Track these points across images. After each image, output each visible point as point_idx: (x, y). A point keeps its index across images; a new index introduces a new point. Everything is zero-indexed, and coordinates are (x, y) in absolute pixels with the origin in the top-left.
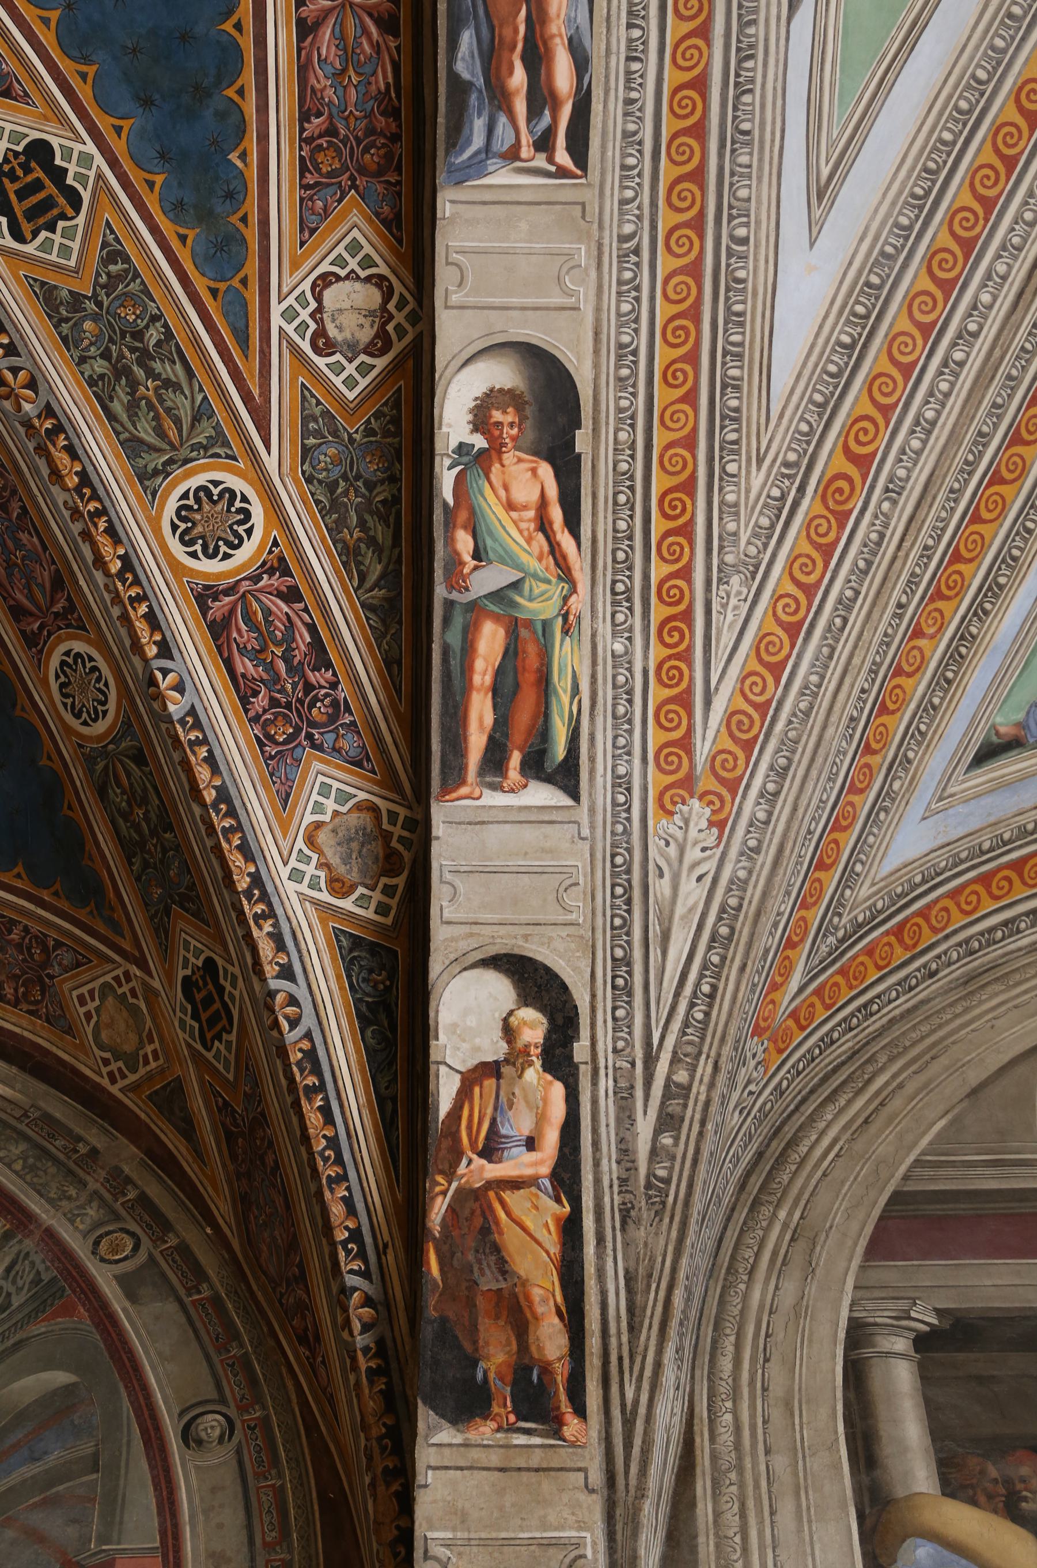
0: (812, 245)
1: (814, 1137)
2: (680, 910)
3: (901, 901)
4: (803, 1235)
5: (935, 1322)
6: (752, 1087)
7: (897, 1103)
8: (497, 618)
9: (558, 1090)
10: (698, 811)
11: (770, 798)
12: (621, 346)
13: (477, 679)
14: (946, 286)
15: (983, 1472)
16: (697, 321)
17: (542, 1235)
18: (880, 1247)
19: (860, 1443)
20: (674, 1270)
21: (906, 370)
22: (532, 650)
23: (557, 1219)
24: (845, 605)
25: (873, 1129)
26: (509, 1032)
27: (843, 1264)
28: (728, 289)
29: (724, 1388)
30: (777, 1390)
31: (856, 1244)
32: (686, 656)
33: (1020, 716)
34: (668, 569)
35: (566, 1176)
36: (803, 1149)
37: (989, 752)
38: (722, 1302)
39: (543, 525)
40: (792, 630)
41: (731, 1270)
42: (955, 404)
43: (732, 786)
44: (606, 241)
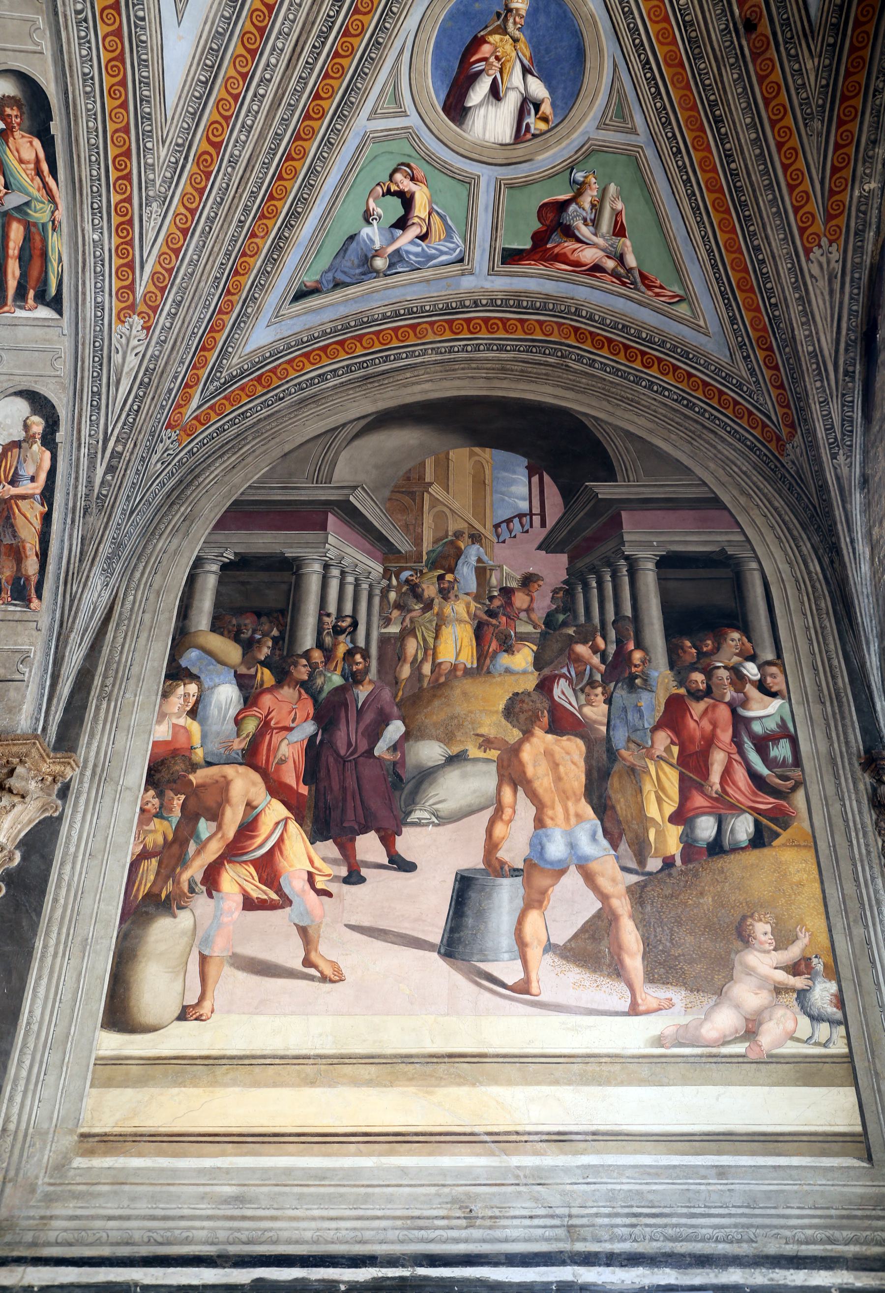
0: (179, 24)
2: (126, 370)
3: (257, 365)
4: (189, 519)
6: (171, 452)
7: (250, 459)
8: (19, 221)
9: (48, 455)
10: (137, 321)
11: (172, 316)
12: (84, 74)
13: (11, 252)
14: (253, 53)
16: (123, 63)
17: (33, 521)
18: (221, 525)
20: (102, 536)
21: (236, 97)
22: (37, 238)
23: (41, 514)
24: (211, 220)
25: (235, 471)
26: (26, 427)
28: (137, 46)
29: (133, 585)
30: (156, 586)
32: (131, 243)
33: (318, 277)
34: (120, 197)
35: (48, 495)
37: (301, 295)
38: (144, 548)
39: (39, 172)
40: (184, 232)
41: (153, 533)
42: (261, 117)
43: (154, 310)
44: (68, 13)
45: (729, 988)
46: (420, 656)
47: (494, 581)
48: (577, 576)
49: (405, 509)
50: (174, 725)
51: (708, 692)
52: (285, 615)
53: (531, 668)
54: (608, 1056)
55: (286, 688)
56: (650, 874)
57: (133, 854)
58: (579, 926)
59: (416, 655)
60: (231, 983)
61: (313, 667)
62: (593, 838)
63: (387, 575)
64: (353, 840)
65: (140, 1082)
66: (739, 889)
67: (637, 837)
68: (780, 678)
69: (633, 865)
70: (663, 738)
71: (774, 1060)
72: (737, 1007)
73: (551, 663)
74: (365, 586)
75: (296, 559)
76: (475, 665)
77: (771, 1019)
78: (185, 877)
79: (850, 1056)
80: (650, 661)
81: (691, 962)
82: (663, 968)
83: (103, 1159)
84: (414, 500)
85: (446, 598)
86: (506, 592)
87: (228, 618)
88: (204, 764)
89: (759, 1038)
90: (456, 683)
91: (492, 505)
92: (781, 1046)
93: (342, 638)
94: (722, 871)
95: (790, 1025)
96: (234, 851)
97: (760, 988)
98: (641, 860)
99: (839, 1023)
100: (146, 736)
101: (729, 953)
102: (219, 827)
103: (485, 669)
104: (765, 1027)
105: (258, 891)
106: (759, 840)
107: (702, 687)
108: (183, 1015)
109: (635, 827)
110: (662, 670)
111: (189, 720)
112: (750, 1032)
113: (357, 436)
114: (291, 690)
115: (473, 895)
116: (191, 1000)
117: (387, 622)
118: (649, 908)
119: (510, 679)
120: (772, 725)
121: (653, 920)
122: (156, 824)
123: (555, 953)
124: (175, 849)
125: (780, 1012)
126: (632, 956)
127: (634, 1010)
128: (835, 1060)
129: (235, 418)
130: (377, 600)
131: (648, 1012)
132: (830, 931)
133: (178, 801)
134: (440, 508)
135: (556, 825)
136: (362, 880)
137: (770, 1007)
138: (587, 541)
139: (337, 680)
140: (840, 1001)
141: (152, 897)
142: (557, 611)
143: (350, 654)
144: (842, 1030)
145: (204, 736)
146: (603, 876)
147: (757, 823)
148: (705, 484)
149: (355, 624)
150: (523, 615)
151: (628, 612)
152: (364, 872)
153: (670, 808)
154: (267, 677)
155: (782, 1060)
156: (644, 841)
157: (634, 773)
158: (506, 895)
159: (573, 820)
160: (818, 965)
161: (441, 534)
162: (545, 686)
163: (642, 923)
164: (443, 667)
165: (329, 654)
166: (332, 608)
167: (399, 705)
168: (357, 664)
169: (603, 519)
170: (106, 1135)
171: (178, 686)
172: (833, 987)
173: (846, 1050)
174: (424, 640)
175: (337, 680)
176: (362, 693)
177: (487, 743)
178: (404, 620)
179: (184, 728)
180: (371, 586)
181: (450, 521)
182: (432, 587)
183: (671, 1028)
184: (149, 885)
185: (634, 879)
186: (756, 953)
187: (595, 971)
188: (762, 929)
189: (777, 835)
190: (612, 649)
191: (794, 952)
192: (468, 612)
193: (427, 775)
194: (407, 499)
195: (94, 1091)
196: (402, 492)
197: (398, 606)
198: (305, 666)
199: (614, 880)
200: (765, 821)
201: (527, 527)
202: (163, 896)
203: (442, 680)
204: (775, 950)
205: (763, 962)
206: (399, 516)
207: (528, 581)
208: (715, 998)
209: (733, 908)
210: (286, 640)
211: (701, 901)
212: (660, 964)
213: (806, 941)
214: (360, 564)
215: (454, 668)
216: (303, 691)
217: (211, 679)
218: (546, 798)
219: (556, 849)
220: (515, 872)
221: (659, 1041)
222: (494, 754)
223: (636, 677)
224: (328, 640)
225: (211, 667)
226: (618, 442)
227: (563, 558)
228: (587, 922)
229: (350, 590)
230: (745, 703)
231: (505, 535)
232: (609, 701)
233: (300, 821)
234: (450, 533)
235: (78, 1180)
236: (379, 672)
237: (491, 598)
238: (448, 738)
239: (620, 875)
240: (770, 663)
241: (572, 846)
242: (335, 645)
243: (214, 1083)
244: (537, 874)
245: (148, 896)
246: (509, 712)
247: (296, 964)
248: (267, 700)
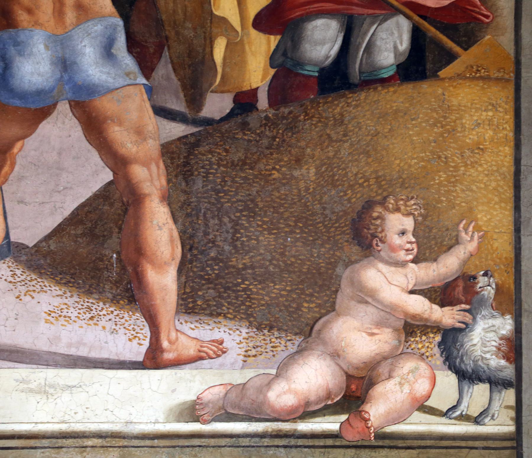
45: (325, 325)
54: (99, 435)
56: (208, 122)
58: (67, 213)
62: (108, 52)
66: (367, 154)
67: (191, 52)
69: (178, 105)
71: (387, 442)
72: (335, 355)
77: (390, 377)
81: (265, 278)
82: (209, 290)
89: (367, 407)
92: (401, 419)
94: (340, 121)
95: (422, 387)
97: (380, 324)
98: (195, 96)
99: (506, 384)
101: (333, 265)
104: (379, 389)
106: (417, 65)
109: (189, 33)
118: (199, 184)
121: (204, 206)
123: (17, 260)
125: (407, 366)
126: (160, 267)
127: (154, 360)
128: (490, 444)
131: (177, 363)
132: (517, 230)
135: (37, 24)
137: (392, 357)
140: (513, 348)
144: (509, 396)
146: (120, 124)
147: (417, 34)
155: (400, 443)
156: (203, 62)
159: (70, 16)
160: (486, 288)
163: (184, 212)
172: (505, 325)
173: (512, 428)
183: (216, 390)
185: (176, 130)
186: (381, 266)
187: (89, 293)
188: (398, 226)
189: (451, 57)
191: (449, 265)
199: (139, 132)
200: (432, 31)
204: (415, 261)
205: (392, 281)
208: (298, 340)
209: (351, 187)
211: (296, 173)
212: (209, 281)
213: (472, 246)
221: (192, 411)
228: (82, 206)
239: (151, 121)
241: (65, 65)
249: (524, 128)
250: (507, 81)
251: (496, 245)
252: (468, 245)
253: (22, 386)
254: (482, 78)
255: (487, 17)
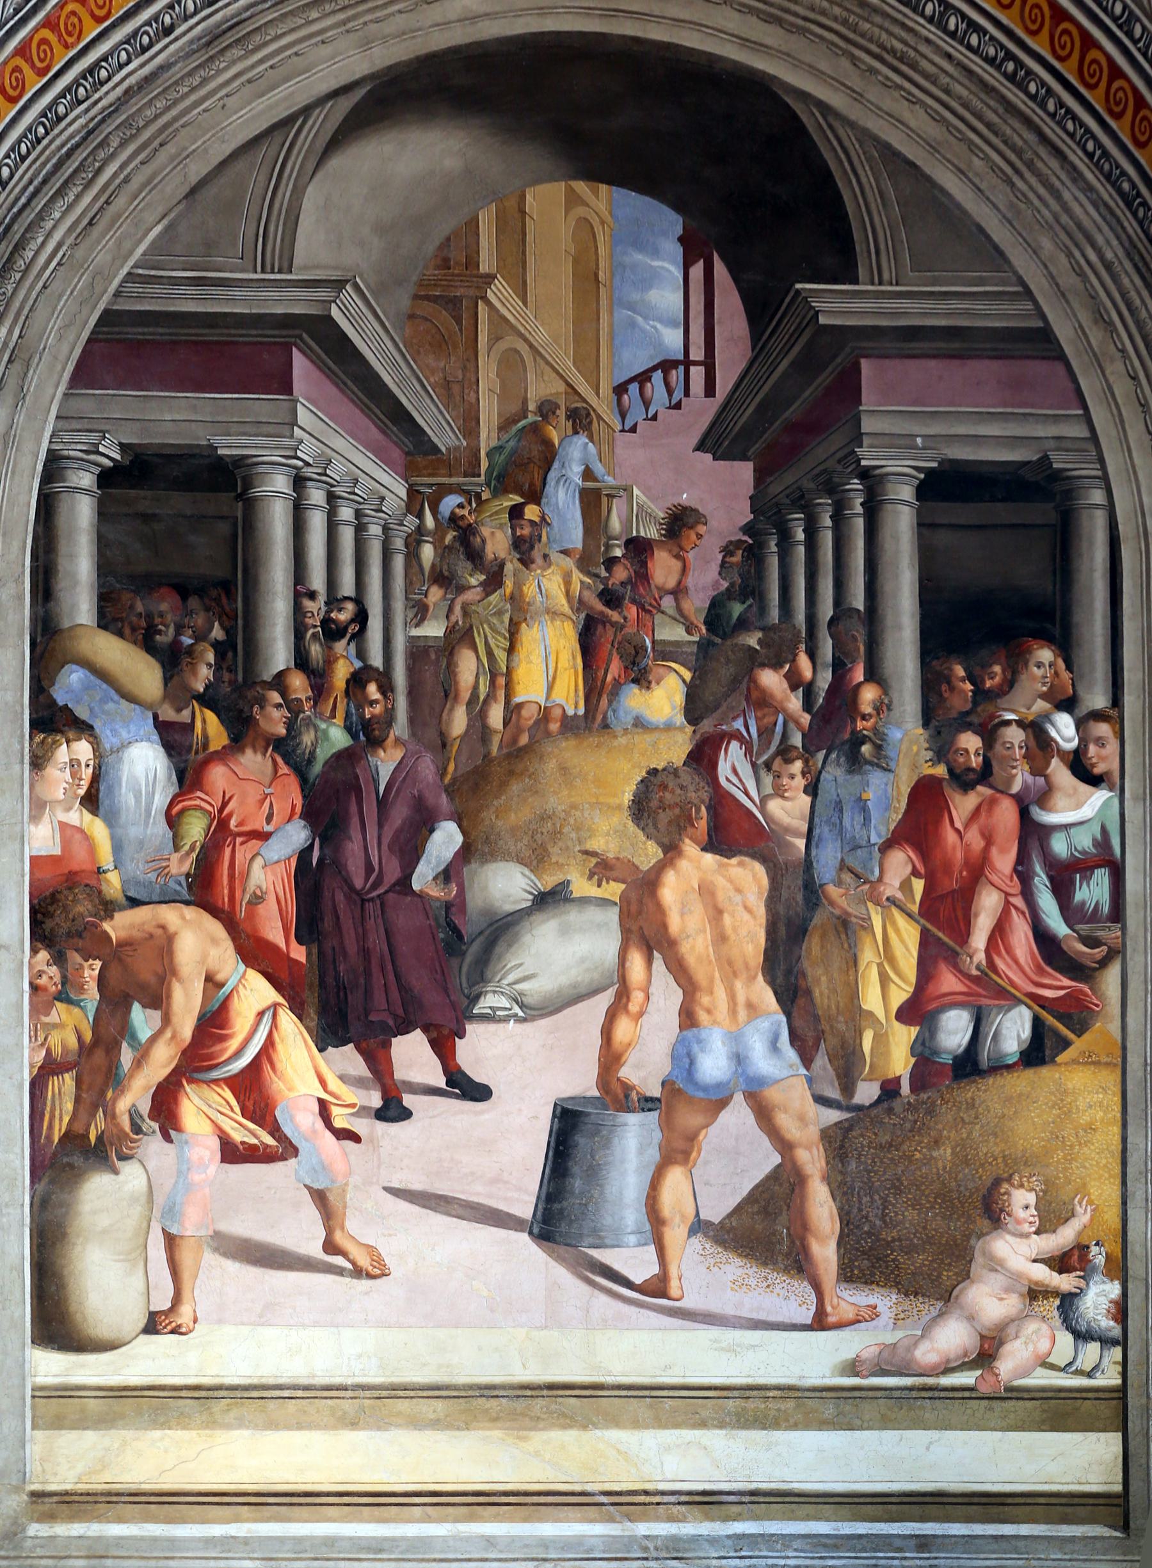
1: (40, 240)
5: (118, 457)
7: (120, 202)
15: (132, 607)
18: (84, 375)
19: (41, 577)
25: (96, 231)
27: (51, 391)
31: (64, 370)
36: (29, 254)
45: (961, 1292)
46: (483, 690)
47: (615, 524)
48: (768, 517)
49: (441, 344)
50: (63, 826)
51: (985, 774)
52: (227, 591)
53: (680, 719)
54: (778, 1388)
55: (249, 752)
56: (859, 1108)
57: (32, 1066)
58: (745, 1193)
59: (476, 687)
60: (217, 1280)
61: (293, 707)
62: (774, 1046)
63: (414, 502)
64: (387, 1045)
65: (103, 1422)
66: (995, 1135)
67: (843, 1044)
68: (1113, 747)
69: (834, 1093)
70: (900, 863)
71: (1015, 1394)
72: (971, 1318)
73: (717, 708)
74: (375, 530)
75: (240, 462)
76: (581, 711)
77: (1017, 1337)
78: (123, 1105)
79: (1123, 1389)
80: (889, 709)
81: (910, 1250)
82: (867, 1261)
83: (70, 1526)
84: (458, 321)
85: (526, 562)
86: (639, 548)
87: (126, 597)
88: (123, 901)
89: (997, 1364)
90: (548, 747)
91: (612, 337)
92: (1026, 1374)
93: (340, 646)
94: (972, 1105)
95: (1044, 1345)
96: (196, 1061)
97: (1008, 1290)
98: (848, 1088)
99: (1114, 1342)
100: (17, 846)
101: (968, 1238)
102: (166, 1020)
103: (599, 718)
104: (1007, 1348)
105: (243, 1132)
106: (1037, 1053)
107: (976, 762)
108: (153, 1325)
109: (842, 1027)
110: (909, 726)
111: (87, 816)
112: (986, 1353)
113: (336, 142)
114: (259, 757)
115: (581, 1141)
116: (162, 1303)
117: (420, 612)
118: (853, 1165)
119: (643, 740)
120: (1084, 841)
121: (858, 1185)
122: (60, 1012)
123: (706, 1235)
124: (99, 1056)
125: (1031, 1327)
126: (822, 1241)
127: (820, 1323)
128: (1101, 1395)
129: (76, 83)
130: (399, 562)
131: (839, 1326)
132: (1124, 1203)
133: (91, 971)
134: (510, 342)
135: (715, 1022)
136: (405, 1114)
137: (1018, 1319)
138: (792, 425)
139: (338, 737)
140: (1121, 1311)
141: (73, 1139)
142: (729, 594)
143: (357, 681)
144: (1117, 1353)
145: (117, 848)
146: (786, 1112)
147: (1037, 1023)
148: (1028, 293)
149: (362, 617)
150: (668, 602)
151: (858, 601)
152: (408, 1100)
153: (900, 995)
154: (211, 727)
155: (1026, 1395)
156: (853, 1053)
157: (847, 929)
158: (633, 1141)
159: (742, 1014)
160: (1097, 1255)
161: (514, 408)
162: (703, 756)
163: (841, 1190)
164: (525, 713)
165: (319, 679)
166: (317, 581)
167: (451, 791)
168: (372, 703)
169: (825, 378)
170: (67, 1493)
171: (56, 744)
172: (1114, 1290)
173: (1119, 1381)
174: (490, 654)
175: (338, 737)
176: (385, 763)
177: (603, 869)
178: (450, 610)
179: (80, 830)
180: (386, 529)
181: (531, 377)
182: (499, 535)
183: (872, 1349)
184: (66, 1119)
185: (833, 1116)
186: (1008, 1237)
187: (765, 1264)
188: (1022, 1201)
189: (1066, 1044)
190: (825, 679)
191: (1065, 1237)
192: (568, 594)
193: (503, 928)
194: (444, 318)
195: (39, 1434)
196: (434, 299)
197: (443, 578)
198: (278, 706)
199: (802, 1119)
200: (1050, 1020)
201: (678, 394)
202: (93, 1137)
203: (524, 740)
204: (1037, 1233)
205: (1018, 1251)
206: (431, 360)
207: (680, 523)
208: (939, 1304)
209: (982, 1165)
210: (240, 648)
211: (935, 1154)
212: (863, 1253)
213: (1086, 1219)
214: (363, 479)
215: (545, 715)
216: (279, 760)
217: (114, 732)
218: (700, 974)
219: (713, 1065)
220: (648, 1103)
221: (853, 1367)
222: (613, 890)
223: (863, 740)
224: (315, 650)
225: (110, 706)
226: (867, 177)
227: (745, 471)
228: (757, 1187)
229: (347, 536)
230: (1044, 798)
231: (637, 414)
232: (812, 789)
233: (298, 1009)
234: (532, 407)
235: (39, 1552)
236: (412, 721)
237: (610, 563)
238: (536, 859)
239: (813, 1110)
240: (1098, 716)
241: (739, 1059)
242: (330, 661)
243: (212, 1424)
244: (682, 1107)
245: (67, 1137)
246: (641, 809)
247: (314, 1249)
248: (218, 775)
249: (1129, 1109)
250: (1115, 1065)
251: (1106, 1217)
252: (1083, 1217)
253: (716, 1345)
254: (1093, 1063)
255: (1097, 1006)
